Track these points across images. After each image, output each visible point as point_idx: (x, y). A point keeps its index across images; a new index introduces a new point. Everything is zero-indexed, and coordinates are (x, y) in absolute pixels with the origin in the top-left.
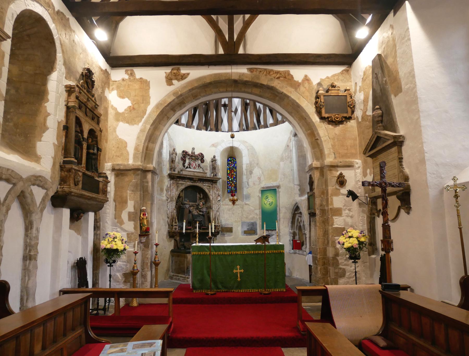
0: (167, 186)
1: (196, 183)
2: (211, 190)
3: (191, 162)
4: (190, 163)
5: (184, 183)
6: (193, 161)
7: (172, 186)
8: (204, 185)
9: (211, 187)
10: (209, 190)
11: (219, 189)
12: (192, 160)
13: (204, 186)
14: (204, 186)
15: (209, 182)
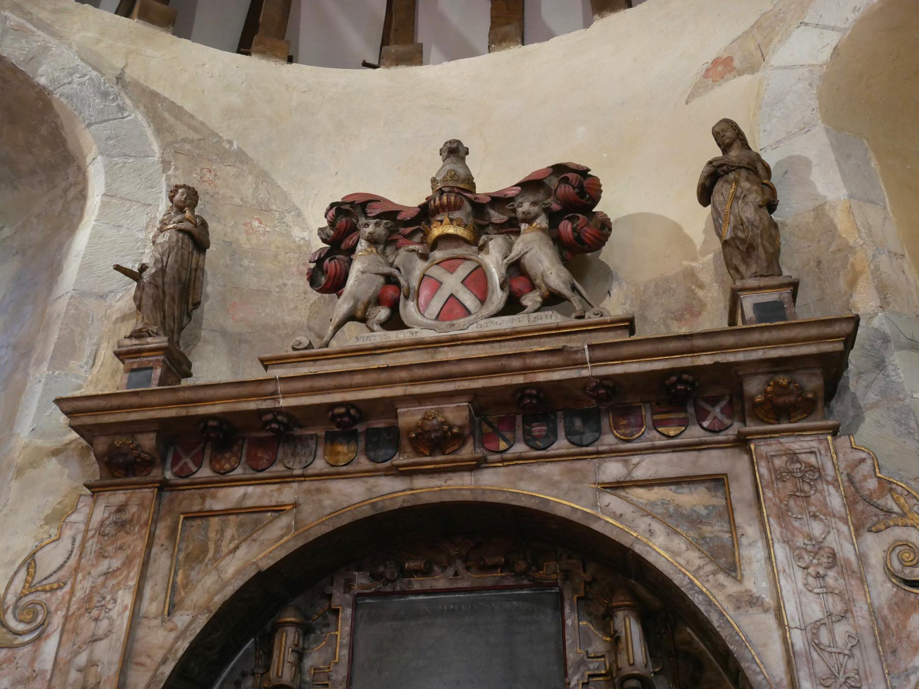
0: (31, 562)
1: (477, 465)
2: (751, 531)
3: (420, 266)
4: (390, 280)
5: (287, 494)
6: (438, 255)
7: (102, 555)
8: (613, 470)
9: (741, 490)
10: (717, 530)
11: (886, 486)
12: (434, 246)
13: (617, 486)
14: (617, 486)
15: (685, 423)
